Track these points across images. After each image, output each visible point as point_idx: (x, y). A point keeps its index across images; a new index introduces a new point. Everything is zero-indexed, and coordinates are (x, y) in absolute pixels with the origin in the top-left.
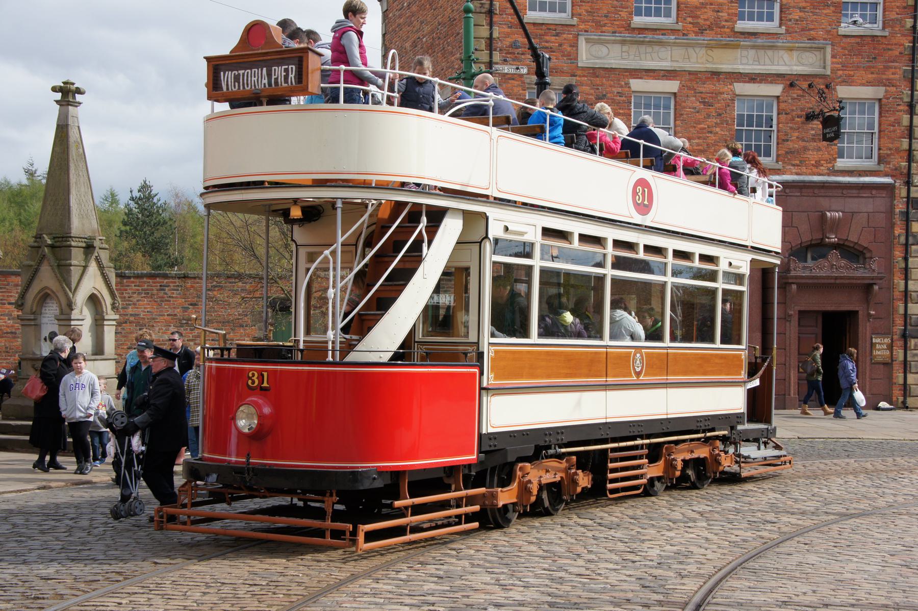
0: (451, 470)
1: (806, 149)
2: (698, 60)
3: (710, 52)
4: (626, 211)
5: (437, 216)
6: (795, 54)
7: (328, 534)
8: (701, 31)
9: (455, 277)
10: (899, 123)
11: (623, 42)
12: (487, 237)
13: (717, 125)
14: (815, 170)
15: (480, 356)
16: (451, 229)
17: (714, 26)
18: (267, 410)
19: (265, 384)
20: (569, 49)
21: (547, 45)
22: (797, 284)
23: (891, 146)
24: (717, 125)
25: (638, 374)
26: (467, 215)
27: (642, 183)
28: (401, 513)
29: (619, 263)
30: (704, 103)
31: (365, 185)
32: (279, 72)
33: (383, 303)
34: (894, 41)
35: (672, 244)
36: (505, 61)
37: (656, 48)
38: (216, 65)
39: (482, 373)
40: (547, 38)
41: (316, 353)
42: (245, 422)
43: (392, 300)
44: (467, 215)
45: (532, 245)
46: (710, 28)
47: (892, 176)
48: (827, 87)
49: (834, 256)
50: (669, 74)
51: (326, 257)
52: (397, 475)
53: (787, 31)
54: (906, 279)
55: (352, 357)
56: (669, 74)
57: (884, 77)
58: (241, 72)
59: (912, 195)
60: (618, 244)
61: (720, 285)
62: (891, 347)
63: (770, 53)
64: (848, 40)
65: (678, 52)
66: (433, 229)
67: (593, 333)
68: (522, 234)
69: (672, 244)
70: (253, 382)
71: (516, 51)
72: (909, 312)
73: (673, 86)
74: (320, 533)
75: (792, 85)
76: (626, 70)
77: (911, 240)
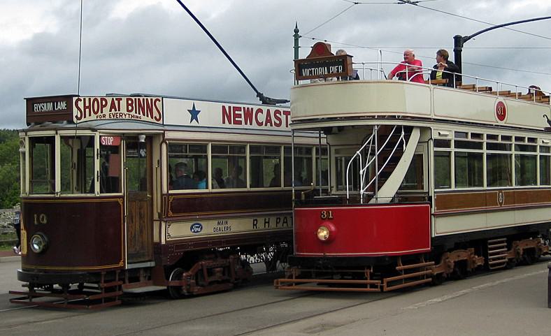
0: (419, 254)
4: (493, 119)
5: (409, 130)
7: (369, 286)
9: (418, 160)
12: (431, 138)
15: (430, 198)
16: (415, 135)
18: (333, 228)
19: (331, 217)
25: (501, 204)
26: (423, 130)
27: (500, 103)
28: (398, 273)
29: (490, 146)
31: (373, 118)
32: (334, 69)
33: (385, 176)
35: (514, 134)
38: (300, 66)
39: (431, 207)
41: (354, 200)
42: (323, 234)
43: (390, 174)
44: (423, 130)
45: (450, 141)
51: (358, 155)
52: (394, 258)
55: (373, 201)
58: (313, 69)
60: (489, 137)
61: (538, 153)
66: (407, 137)
67: (476, 184)
68: (446, 135)
69: (514, 134)
70: (324, 216)
74: (365, 286)
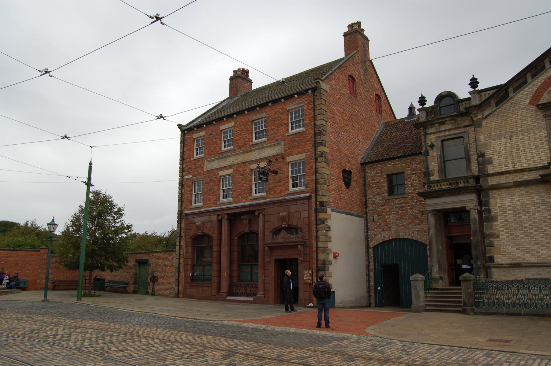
1: (276, 187)
6: (272, 148)
10: (311, 167)
11: (218, 159)
13: (245, 183)
14: (280, 195)
22: (268, 247)
24: (245, 183)
36: (187, 175)
46: (243, 146)
49: (283, 232)
50: (230, 167)
53: (268, 140)
54: (317, 242)
56: (230, 167)
62: (312, 275)
63: (263, 150)
64: (289, 137)
65: (234, 158)
72: (319, 258)
73: (230, 171)
76: (218, 169)
77: (319, 222)
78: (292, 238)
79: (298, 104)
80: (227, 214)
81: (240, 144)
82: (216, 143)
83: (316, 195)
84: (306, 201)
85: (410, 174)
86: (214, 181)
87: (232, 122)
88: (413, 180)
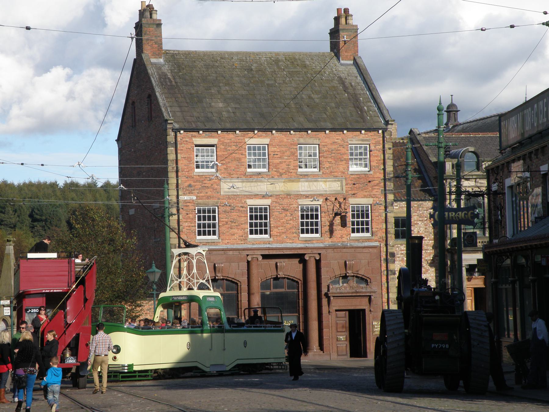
2: (280, 187)
3: (286, 185)
8: (281, 174)
11: (243, 182)
17: (288, 172)
20: (216, 187)
21: (206, 185)
23: (377, 227)
30: (284, 209)
34: (375, 176)
36: (184, 194)
37: (259, 184)
40: (205, 182)
47: (379, 241)
48: (345, 199)
53: (323, 173)
57: (372, 193)
59: (389, 251)
71: (190, 189)
75: (326, 199)
76: (245, 195)
77: (389, 273)
78: (363, 288)
79: (363, 140)
80: (261, 255)
81: (281, 171)
82: (239, 160)
83: (386, 245)
84: (375, 250)
85: (417, 221)
86: (239, 210)
87: (266, 137)
88: (420, 227)
